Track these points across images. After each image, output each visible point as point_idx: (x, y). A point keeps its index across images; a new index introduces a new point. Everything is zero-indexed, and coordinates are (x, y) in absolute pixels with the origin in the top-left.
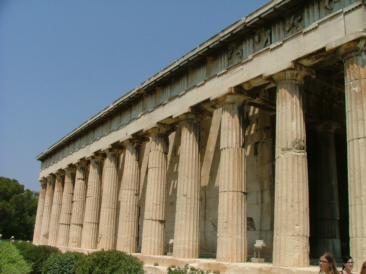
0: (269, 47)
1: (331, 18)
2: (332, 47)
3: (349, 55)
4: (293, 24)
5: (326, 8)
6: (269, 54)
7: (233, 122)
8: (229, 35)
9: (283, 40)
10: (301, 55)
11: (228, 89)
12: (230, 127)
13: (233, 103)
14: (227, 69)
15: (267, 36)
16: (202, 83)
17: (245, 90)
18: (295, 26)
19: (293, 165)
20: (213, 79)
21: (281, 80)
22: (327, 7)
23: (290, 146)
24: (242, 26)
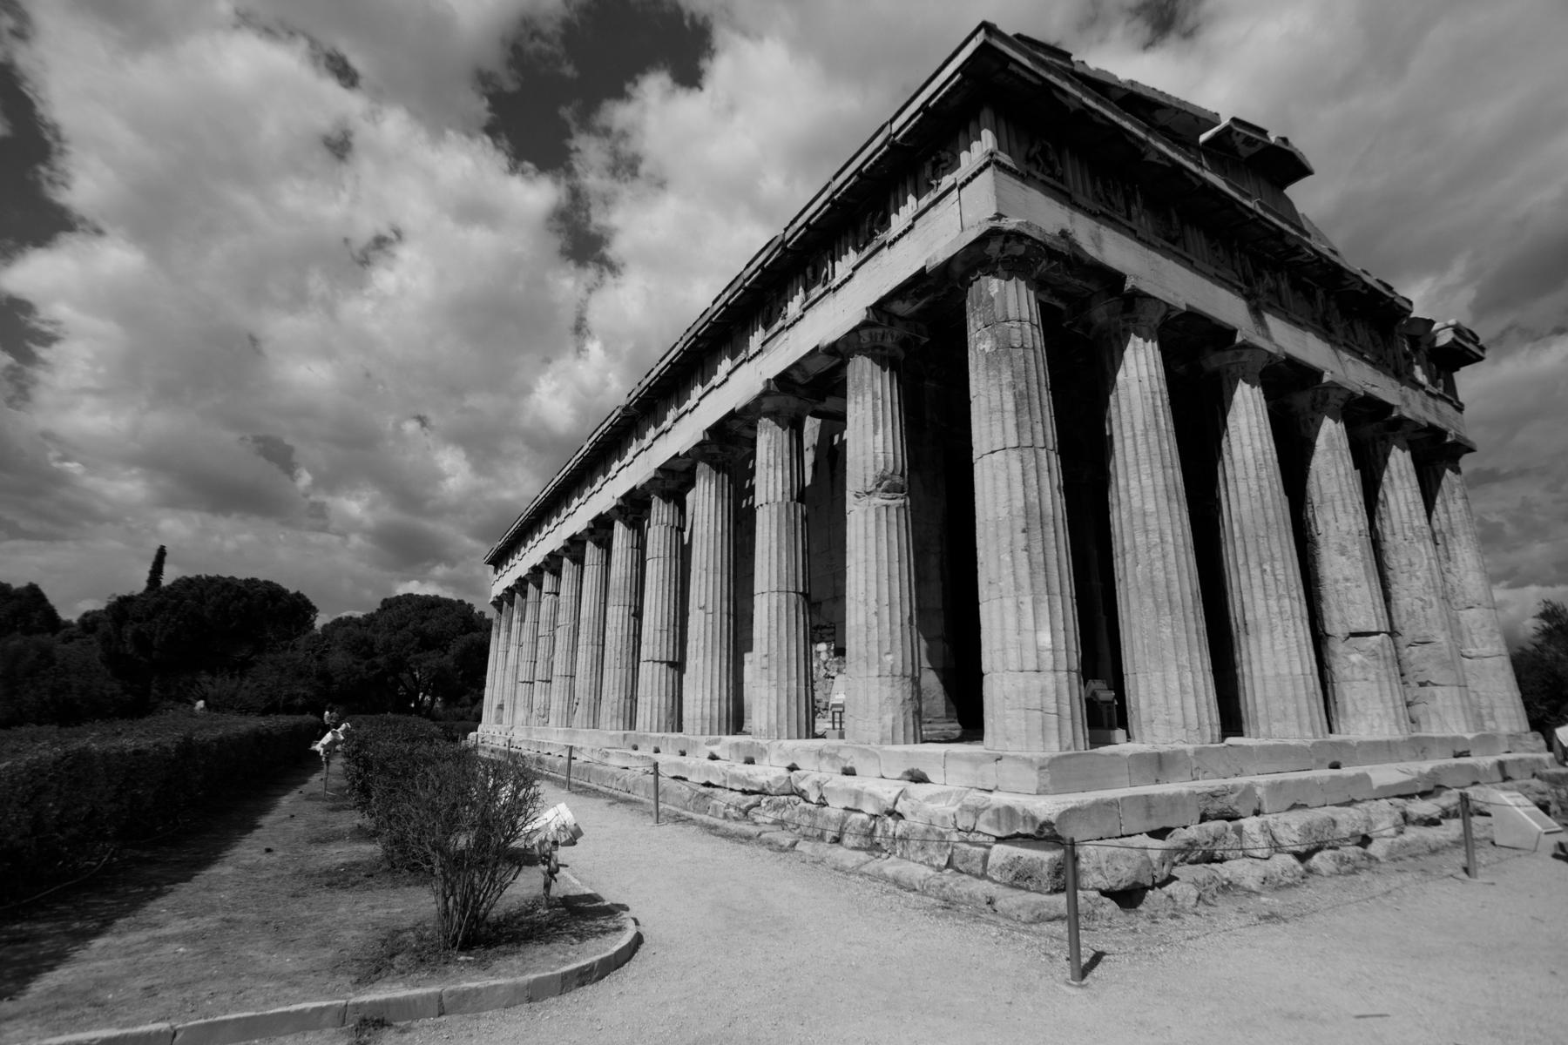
1: (935, 202)
10: (884, 292)
17: (800, 385)
19: (877, 526)
23: (870, 486)
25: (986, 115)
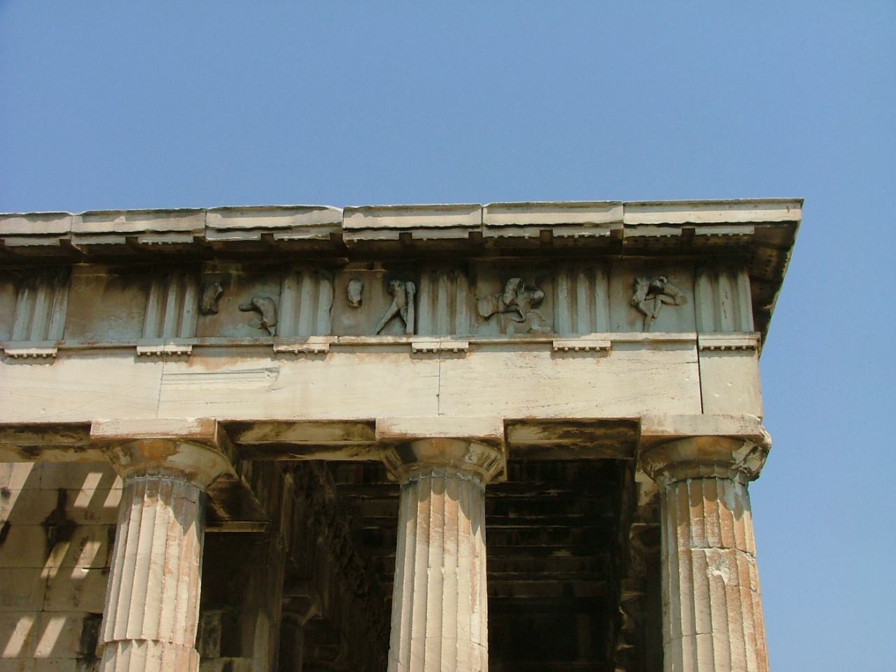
0: (411, 340)
1: (656, 345)
2: (663, 432)
3: (703, 470)
4: (513, 303)
5: (635, 306)
6: (404, 359)
7: (184, 548)
8: (255, 236)
9: (473, 340)
10: (541, 413)
11: (202, 422)
12: (173, 564)
13: (190, 477)
14: (194, 346)
15: (400, 299)
16: (44, 352)
18: (518, 312)
20: (106, 355)
21: (443, 465)
22: (642, 306)
24: (329, 230)
25: (744, 282)
